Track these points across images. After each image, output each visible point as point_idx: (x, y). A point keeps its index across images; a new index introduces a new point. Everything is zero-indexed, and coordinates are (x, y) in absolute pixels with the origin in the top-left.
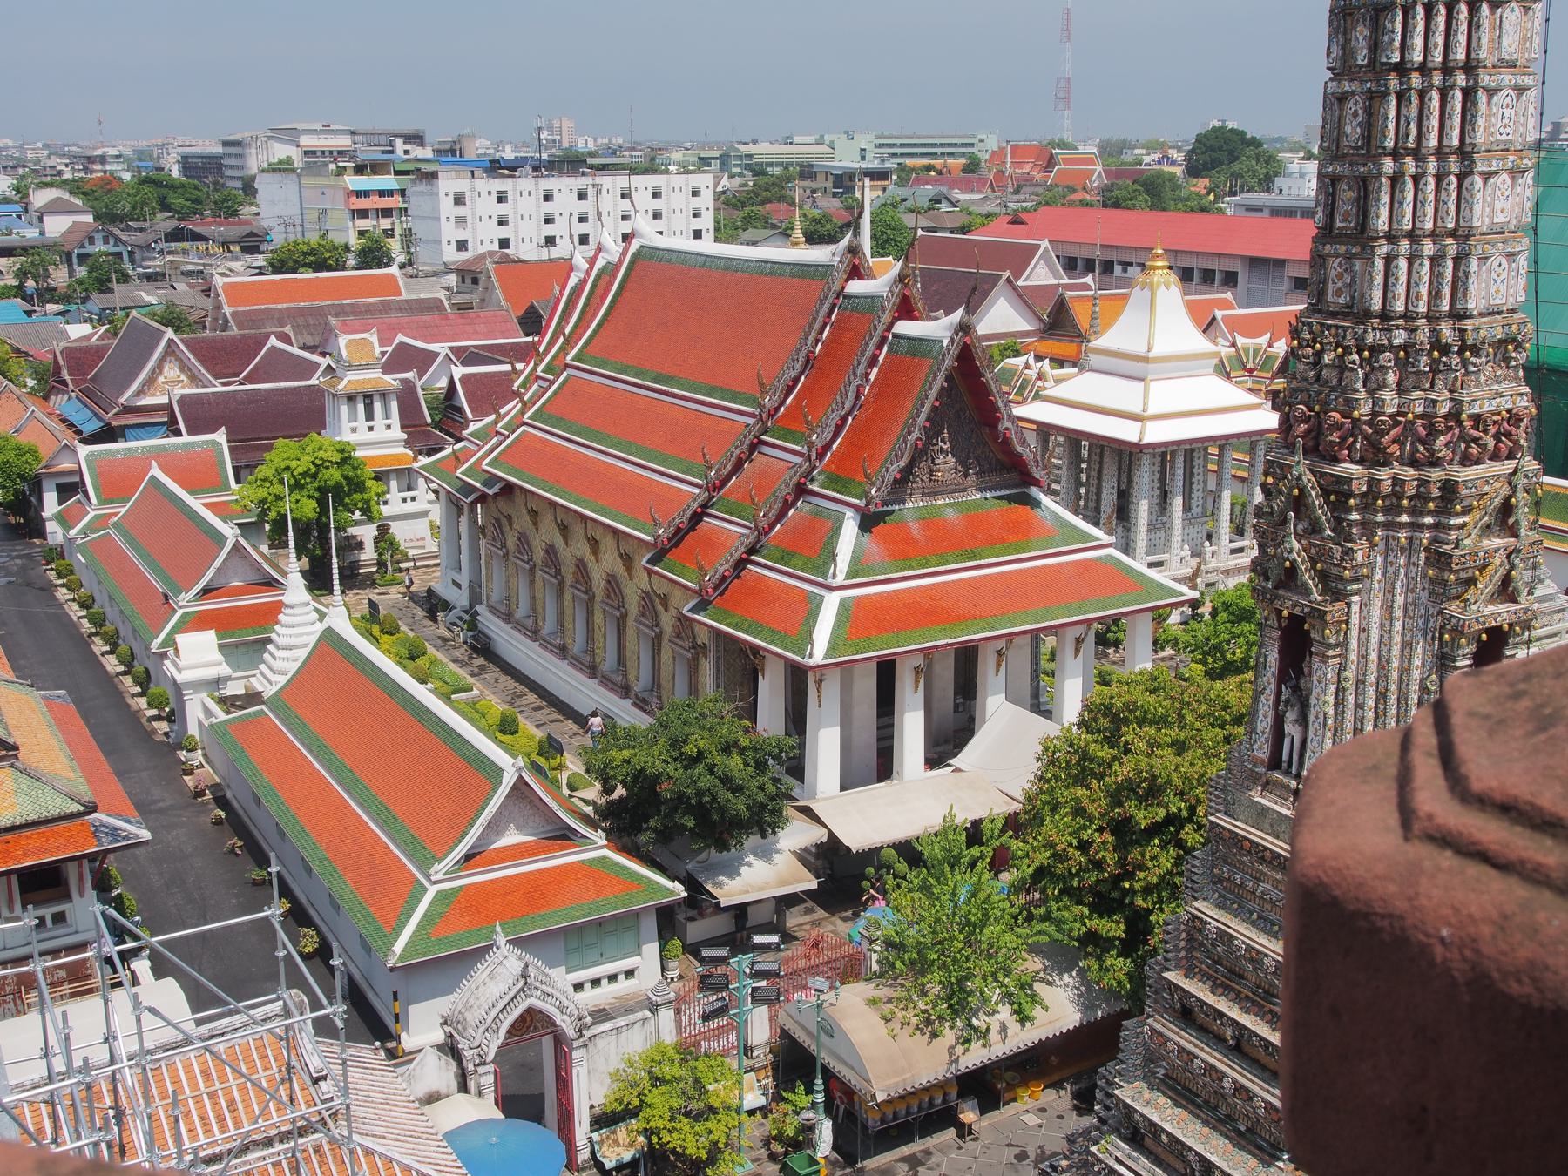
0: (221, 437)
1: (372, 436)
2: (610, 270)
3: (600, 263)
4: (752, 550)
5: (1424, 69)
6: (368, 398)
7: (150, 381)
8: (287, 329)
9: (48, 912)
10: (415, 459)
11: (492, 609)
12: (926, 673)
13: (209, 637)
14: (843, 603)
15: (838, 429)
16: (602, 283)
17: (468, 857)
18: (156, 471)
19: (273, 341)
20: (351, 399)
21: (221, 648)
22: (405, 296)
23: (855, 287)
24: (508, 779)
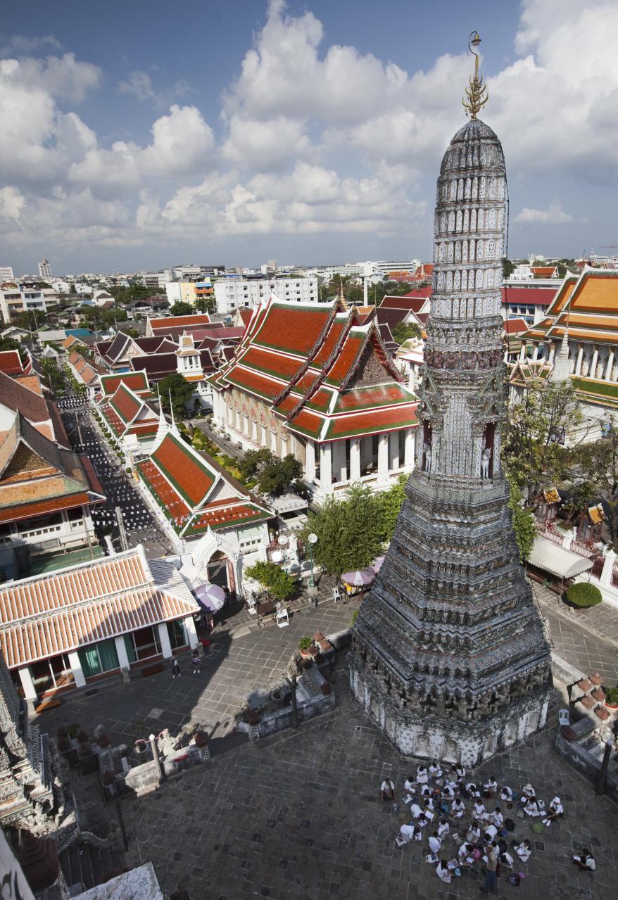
0: (144, 371)
1: (192, 370)
2: (264, 311)
3: (261, 310)
4: (304, 404)
5: (462, 233)
6: (190, 357)
7: (124, 353)
8: (170, 335)
9: (77, 521)
10: (204, 377)
12: (362, 442)
13: (135, 435)
14: (332, 422)
15: (332, 363)
18: (122, 383)
19: (165, 339)
20: (185, 358)
21: (138, 440)
22: (210, 323)
23: (339, 315)
24: (217, 480)
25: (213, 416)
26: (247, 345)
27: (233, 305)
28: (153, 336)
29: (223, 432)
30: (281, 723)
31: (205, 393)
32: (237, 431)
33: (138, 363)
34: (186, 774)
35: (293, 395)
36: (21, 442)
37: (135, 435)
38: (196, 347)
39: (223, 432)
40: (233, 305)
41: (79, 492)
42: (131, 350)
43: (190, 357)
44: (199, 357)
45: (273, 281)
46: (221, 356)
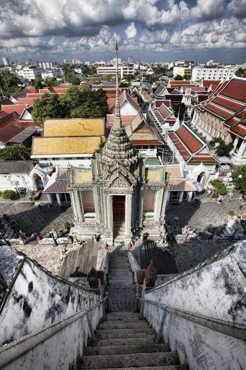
0: (170, 100)
2: (227, 82)
6: (188, 97)
7: (162, 93)
8: (177, 88)
11: (198, 126)
13: (168, 124)
16: (225, 84)
17: (197, 154)
18: (163, 104)
19: (175, 89)
20: (186, 97)
21: (169, 125)
22: (191, 84)
24: (204, 146)
25: (191, 121)
26: (215, 95)
27: (198, 78)
28: (170, 87)
29: (195, 127)
30: (226, 238)
31: (189, 112)
32: (202, 128)
33: (167, 97)
34: (192, 242)
35: (235, 118)
36: (143, 120)
37: (168, 124)
38: (191, 94)
39: (195, 127)
40: (198, 78)
41: (156, 140)
42: (165, 92)
43: (188, 97)
44: (191, 98)
45: (216, 69)
46: (196, 98)
